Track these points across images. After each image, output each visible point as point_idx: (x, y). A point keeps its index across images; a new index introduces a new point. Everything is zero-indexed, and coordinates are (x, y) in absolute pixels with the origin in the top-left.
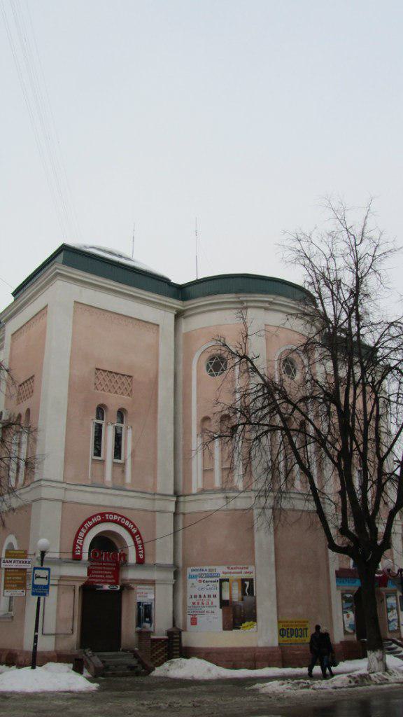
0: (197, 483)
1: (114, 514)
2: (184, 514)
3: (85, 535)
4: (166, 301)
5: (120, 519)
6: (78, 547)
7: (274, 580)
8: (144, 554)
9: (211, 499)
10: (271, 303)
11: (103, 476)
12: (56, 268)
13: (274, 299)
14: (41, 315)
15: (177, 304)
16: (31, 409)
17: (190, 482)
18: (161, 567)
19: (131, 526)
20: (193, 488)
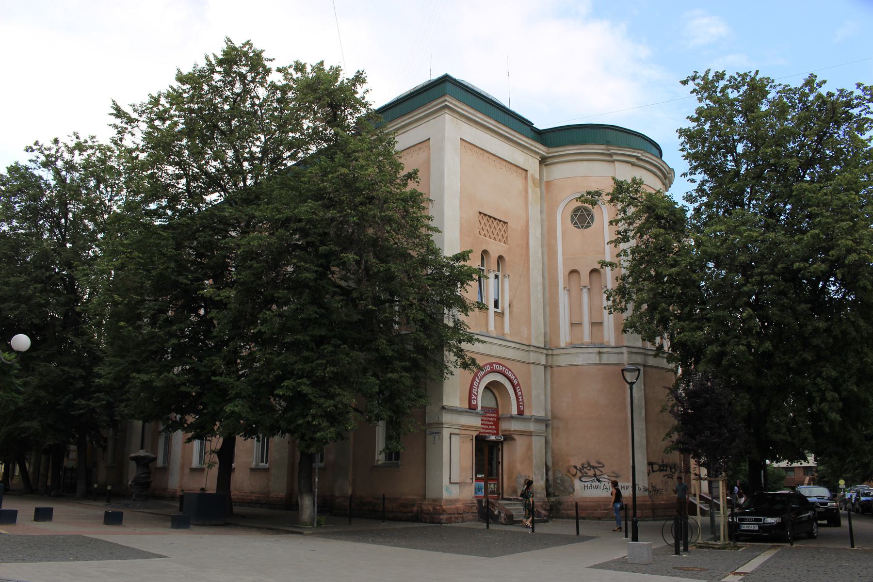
0: (564, 337)
1: (500, 364)
2: (551, 367)
3: (479, 383)
4: (536, 147)
5: (505, 370)
6: (474, 397)
7: (644, 435)
8: (523, 406)
9: (583, 353)
10: (638, 158)
11: (487, 324)
12: (446, 101)
13: (642, 155)
14: (417, 148)
15: (542, 150)
16: (615, 255)
17: (558, 337)
18: (538, 420)
19: (513, 377)
20: (561, 343)
